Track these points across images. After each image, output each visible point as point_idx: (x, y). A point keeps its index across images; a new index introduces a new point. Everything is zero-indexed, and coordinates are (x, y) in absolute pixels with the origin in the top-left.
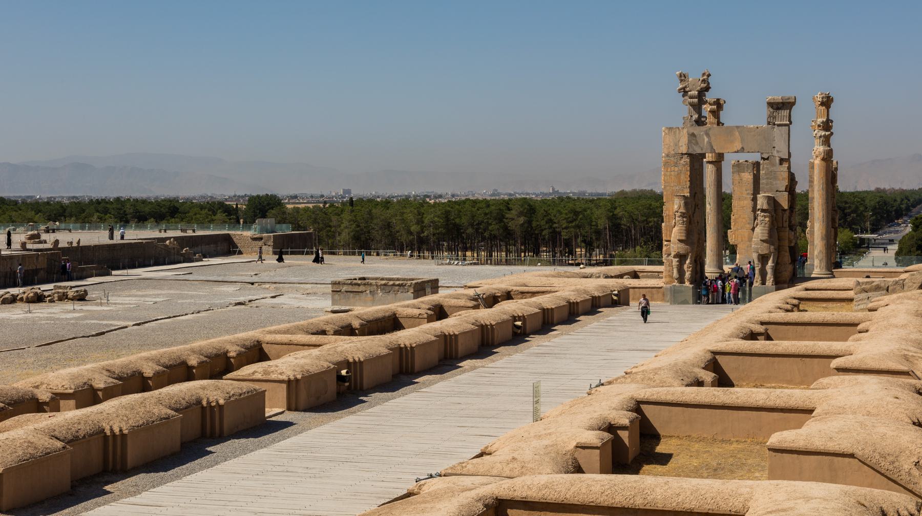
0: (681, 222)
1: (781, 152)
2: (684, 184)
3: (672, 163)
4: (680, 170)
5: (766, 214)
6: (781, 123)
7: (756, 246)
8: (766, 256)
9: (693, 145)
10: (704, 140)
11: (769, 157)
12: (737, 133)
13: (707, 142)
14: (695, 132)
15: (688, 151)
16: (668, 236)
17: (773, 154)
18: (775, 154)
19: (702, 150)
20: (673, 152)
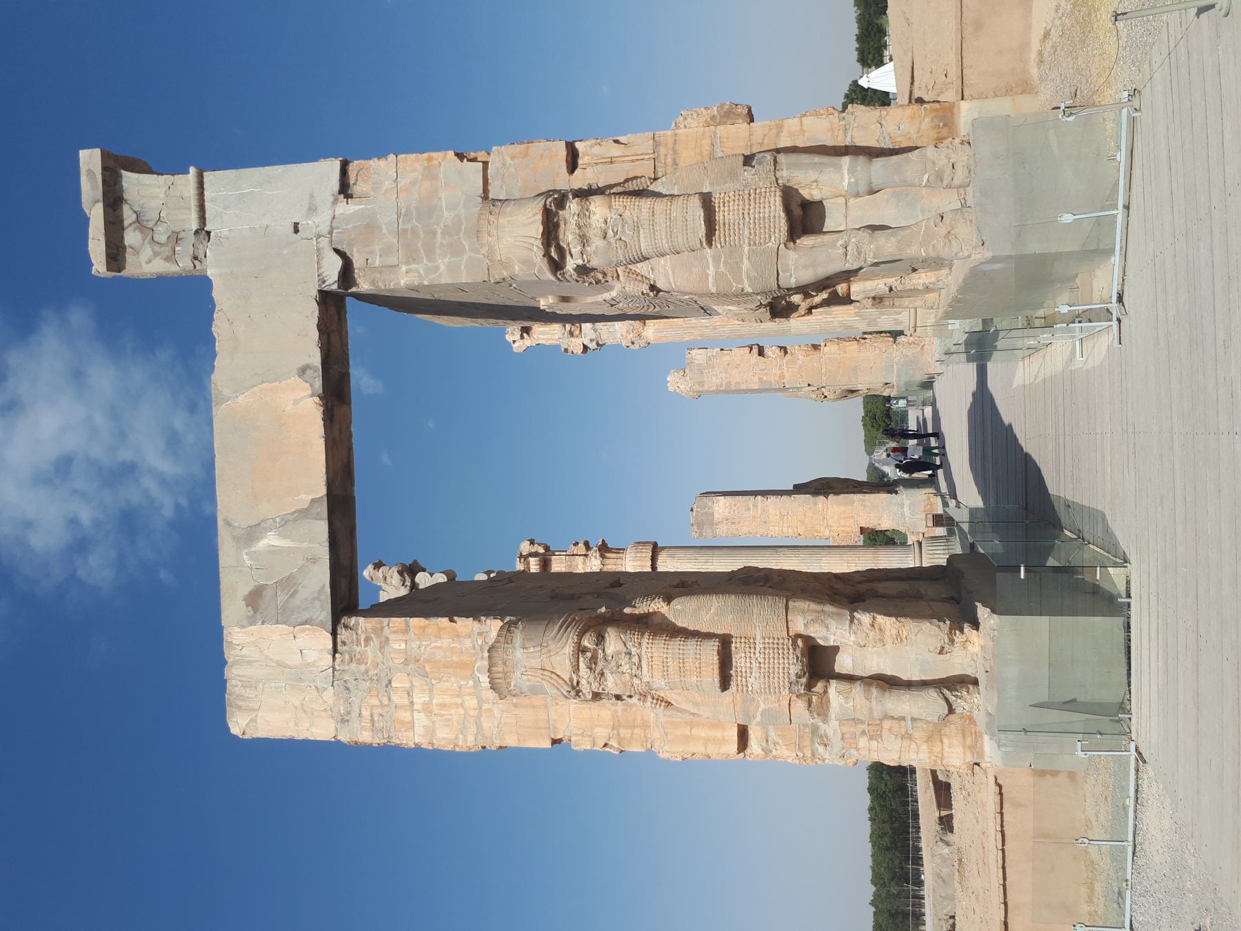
0: (625, 668)
1: (312, 196)
2: (468, 643)
3: (375, 701)
4: (406, 662)
5: (573, 221)
6: (193, 203)
7: (746, 264)
8: (798, 212)
9: (297, 600)
10: (273, 551)
11: (337, 251)
12: (241, 398)
13: (282, 536)
14: (245, 590)
15: (322, 625)
16: (718, 734)
17: (324, 229)
18: (321, 221)
19: (314, 560)
20: (329, 694)
